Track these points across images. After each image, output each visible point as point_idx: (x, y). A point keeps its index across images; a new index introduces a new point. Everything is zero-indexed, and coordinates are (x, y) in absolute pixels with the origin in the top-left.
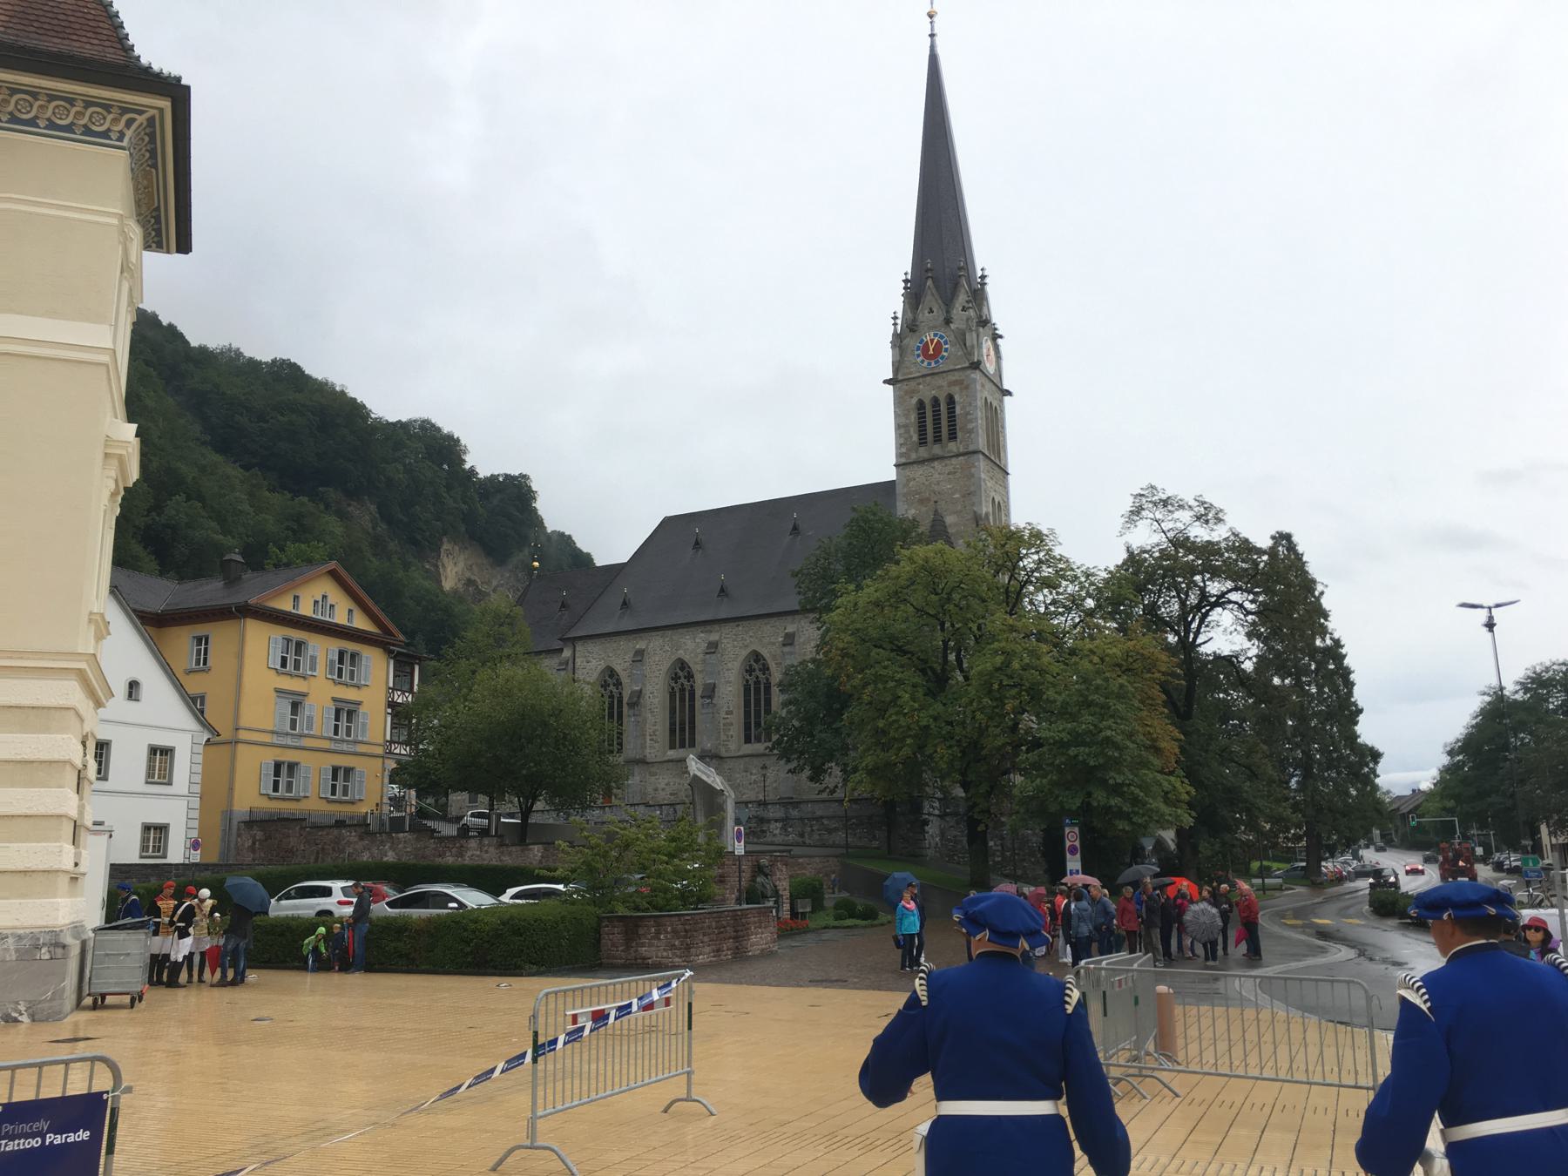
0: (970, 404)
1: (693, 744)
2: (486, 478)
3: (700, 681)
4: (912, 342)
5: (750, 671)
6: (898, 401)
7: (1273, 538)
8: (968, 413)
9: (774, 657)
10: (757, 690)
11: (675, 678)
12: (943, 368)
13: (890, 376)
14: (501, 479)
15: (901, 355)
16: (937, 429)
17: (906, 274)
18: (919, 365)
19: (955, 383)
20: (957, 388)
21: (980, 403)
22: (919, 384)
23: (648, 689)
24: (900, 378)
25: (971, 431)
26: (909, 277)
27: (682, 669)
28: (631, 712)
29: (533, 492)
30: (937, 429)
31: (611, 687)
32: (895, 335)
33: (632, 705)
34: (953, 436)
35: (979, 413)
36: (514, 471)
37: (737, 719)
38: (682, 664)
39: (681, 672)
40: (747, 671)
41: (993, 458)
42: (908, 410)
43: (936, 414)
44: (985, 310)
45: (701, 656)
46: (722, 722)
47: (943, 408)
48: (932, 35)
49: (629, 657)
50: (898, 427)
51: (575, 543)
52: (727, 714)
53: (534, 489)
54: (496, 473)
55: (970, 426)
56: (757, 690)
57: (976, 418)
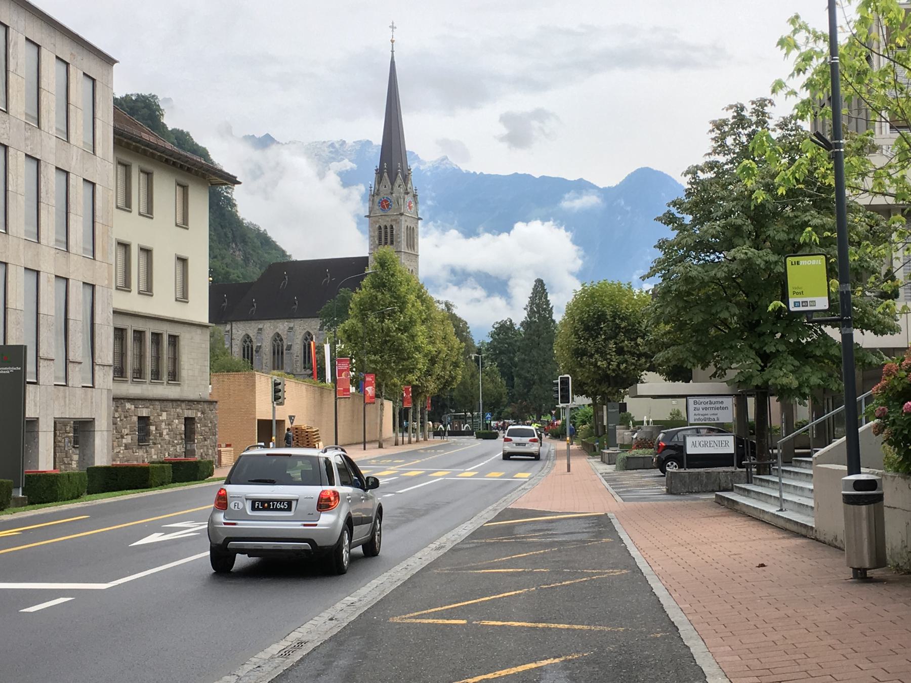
0: (399, 230)
1: (282, 369)
2: (122, 98)
3: (286, 343)
4: (377, 199)
6: (371, 225)
7: (536, 281)
8: (398, 234)
11: (275, 340)
13: (368, 214)
14: (134, 98)
16: (386, 239)
18: (379, 212)
19: (395, 220)
20: (394, 223)
21: (403, 229)
23: (263, 346)
24: (372, 215)
25: (399, 242)
26: (378, 167)
28: (257, 355)
29: (161, 110)
30: (386, 239)
31: (248, 343)
33: (257, 352)
34: (392, 243)
35: (403, 234)
36: (145, 92)
38: (278, 335)
39: (278, 338)
41: (410, 252)
43: (386, 233)
44: (409, 185)
45: (286, 332)
47: (389, 230)
48: (393, 51)
49: (256, 331)
50: (371, 236)
51: (192, 139)
52: (297, 356)
53: (162, 107)
54: (129, 93)
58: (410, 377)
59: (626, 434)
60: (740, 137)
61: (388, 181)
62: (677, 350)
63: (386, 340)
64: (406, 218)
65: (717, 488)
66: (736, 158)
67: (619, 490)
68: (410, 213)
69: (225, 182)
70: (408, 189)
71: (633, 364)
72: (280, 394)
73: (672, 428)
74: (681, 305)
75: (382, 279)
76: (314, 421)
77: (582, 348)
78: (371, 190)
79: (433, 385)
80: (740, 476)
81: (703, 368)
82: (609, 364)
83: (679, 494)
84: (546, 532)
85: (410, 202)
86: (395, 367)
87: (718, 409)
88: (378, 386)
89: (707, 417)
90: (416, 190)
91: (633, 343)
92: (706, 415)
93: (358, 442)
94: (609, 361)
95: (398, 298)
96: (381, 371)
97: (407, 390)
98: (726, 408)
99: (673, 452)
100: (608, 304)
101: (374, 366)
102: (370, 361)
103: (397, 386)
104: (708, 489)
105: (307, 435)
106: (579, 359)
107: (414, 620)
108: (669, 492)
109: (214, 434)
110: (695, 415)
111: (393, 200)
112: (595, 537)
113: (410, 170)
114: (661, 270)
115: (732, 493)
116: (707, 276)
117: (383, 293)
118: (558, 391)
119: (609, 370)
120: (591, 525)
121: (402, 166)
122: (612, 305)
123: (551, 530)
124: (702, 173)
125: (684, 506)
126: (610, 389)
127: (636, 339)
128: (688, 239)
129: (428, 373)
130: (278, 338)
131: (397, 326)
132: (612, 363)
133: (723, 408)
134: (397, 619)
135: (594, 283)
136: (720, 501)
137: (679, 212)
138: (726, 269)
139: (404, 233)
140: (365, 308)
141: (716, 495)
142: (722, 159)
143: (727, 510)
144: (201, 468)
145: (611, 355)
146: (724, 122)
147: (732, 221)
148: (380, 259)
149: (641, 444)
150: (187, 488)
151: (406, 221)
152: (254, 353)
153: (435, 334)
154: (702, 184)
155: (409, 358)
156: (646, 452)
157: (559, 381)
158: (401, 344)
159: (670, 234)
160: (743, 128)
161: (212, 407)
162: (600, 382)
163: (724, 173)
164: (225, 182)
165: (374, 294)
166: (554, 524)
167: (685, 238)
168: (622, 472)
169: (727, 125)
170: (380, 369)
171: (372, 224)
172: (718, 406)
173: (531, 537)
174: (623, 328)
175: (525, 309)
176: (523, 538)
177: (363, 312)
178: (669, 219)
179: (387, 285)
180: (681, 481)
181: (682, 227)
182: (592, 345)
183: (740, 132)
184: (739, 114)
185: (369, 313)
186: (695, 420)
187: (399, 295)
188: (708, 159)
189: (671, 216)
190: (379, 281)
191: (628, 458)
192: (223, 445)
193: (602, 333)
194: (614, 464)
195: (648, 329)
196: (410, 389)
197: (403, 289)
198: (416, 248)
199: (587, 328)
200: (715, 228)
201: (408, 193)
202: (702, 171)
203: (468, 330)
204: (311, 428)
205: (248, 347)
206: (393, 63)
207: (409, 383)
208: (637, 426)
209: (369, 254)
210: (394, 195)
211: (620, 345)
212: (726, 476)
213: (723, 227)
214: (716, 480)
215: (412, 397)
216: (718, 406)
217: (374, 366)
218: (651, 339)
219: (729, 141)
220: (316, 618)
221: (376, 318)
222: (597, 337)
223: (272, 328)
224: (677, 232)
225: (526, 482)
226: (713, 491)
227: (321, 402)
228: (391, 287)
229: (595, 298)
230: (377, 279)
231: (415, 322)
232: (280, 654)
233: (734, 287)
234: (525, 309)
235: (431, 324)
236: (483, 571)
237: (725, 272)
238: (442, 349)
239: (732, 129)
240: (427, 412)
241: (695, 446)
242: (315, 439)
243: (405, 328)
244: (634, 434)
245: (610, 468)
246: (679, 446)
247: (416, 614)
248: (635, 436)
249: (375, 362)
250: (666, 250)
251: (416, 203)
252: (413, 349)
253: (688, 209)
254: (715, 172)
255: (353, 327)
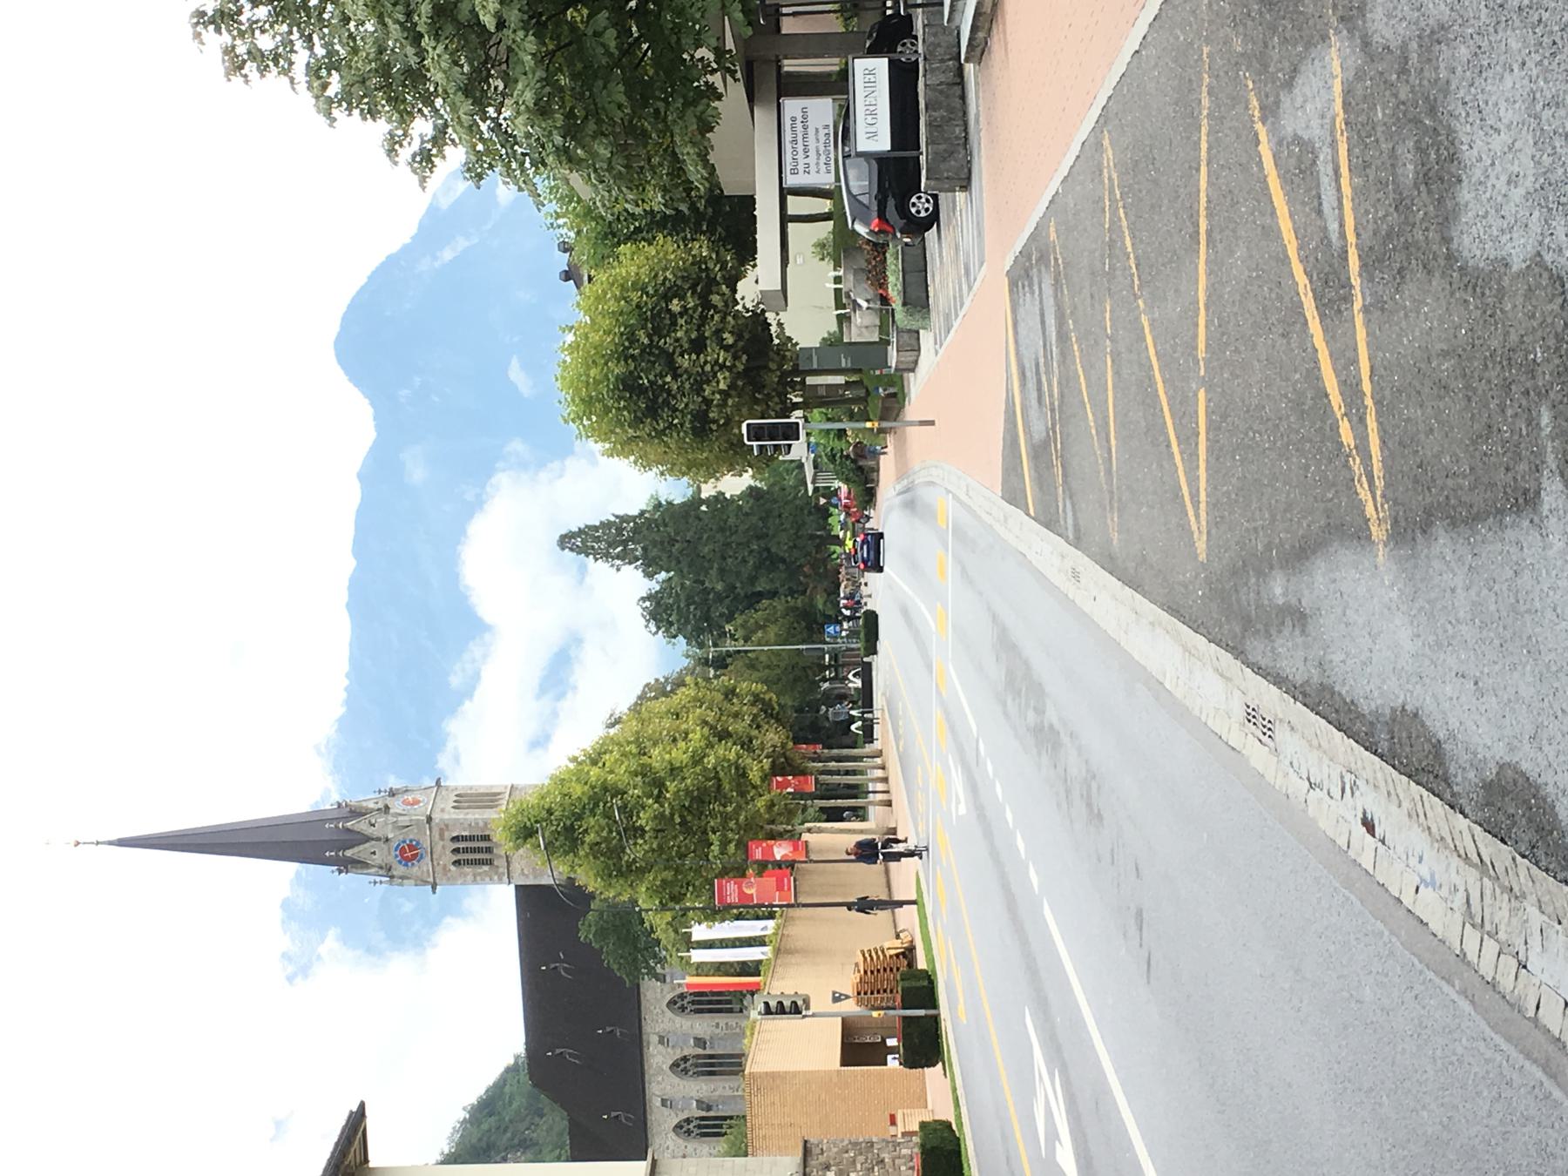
3: (690, 1050)
4: (399, 870)
5: (683, 1009)
6: (451, 880)
7: (563, 549)
8: (470, 825)
9: (673, 989)
10: (700, 1003)
11: (686, 1071)
12: (427, 844)
13: (430, 887)
15: (408, 878)
16: (479, 850)
17: (333, 872)
18: (426, 864)
20: (446, 834)
21: (460, 815)
22: (438, 864)
23: (694, 1094)
24: (431, 880)
27: (678, 1066)
28: (715, 1108)
30: (479, 850)
31: (691, 1126)
32: (391, 883)
34: (486, 838)
35: (469, 816)
37: (722, 1019)
38: (675, 1065)
39: (681, 1067)
40: (683, 1011)
42: (461, 873)
43: (466, 850)
44: (371, 805)
45: (669, 1050)
46: (725, 1031)
47: (461, 845)
48: (98, 843)
49: (666, 1111)
50: (474, 881)
55: (481, 824)
56: (700, 1003)
57: (475, 819)
58: (754, 775)
59: (859, 320)
60: (257, 22)
61: (361, 847)
62: (681, 135)
63: (679, 824)
64: (437, 810)
65: (958, 90)
66: (299, 28)
67: (965, 287)
68: (428, 803)
69: (360, 1133)
70: (376, 807)
71: (723, 320)
72: (787, 1003)
73: (844, 208)
74: (591, 126)
75: (559, 833)
76: (843, 964)
77: (691, 422)
78: (381, 882)
79: (770, 735)
80: (932, 43)
81: (719, 97)
82: (722, 367)
83: (969, 162)
84: (1042, 369)
85: (406, 803)
86: (734, 805)
87: (805, 128)
88: (773, 836)
89: (822, 149)
90: (380, 792)
91: (681, 321)
92: (818, 151)
93: (885, 884)
94: (717, 368)
95: (595, 800)
96: (742, 832)
97: (780, 785)
98: (804, 112)
99: (891, 203)
100: (603, 369)
101: (732, 848)
102: (722, 854)
103: (772, 801)
104: (958, 106)
105: (872, 972)
106: (714, 427)
107: (1203, 506)
108: (966, 185)
109: (872, 1144)
110: (818, 172)
111: (401, 838)
112: (1047, 266)
113: (339, 805)
114: (523, 171)
115: (963, 27)
116: (534, 74)
117: (586, 831)
118: (775, 446)
119: (734, 366)
120: (1027, 289)
121: (331, 820)
122: (606, 364)
123: (1037, 365)
124: (330, 87)
125: (988, 123)
126: (773, 366)
127: (673, 316)
128: (461, 113)
129: (747, 744)
130: (681, 1067)
131: (651, 801)
132: (721, 361)
133: (805, 118)
134: (1201, 545)
135: (563, 400)
136: (979, 50)
137: (410, 144)
138: (521, 34)
139: (468, 813)
140: (615, 865)
141: (967, 60)
142: (301, 58)
143: (994, 25)
144: (935, 1143)
145: (706, 362)
146: (229, 51)
147: (425, 23)
148: (517, 839)
149: (878, 279)
150: (973, 1162)
151: (443, 810)
152: (712, 1114)
153: (669, 732)
154: (352, 86)
155: (717, 777)
156: (893, 267)
157: (755, 444)
158: (688, 792)
159: (455, 156)
160: (239, 12)
161: (816, 1151)
162: (759, 387)
163: (331, 53)
164: (360, 1133)
165: (586, 847)
166: (1027, 366)
167: (459, 118)
168: (933, 314)
169: (233, 47)
170: (738, 833)
171: (449, 879)
172: (799, 126)
173: (1051, 396)
174: (652, 341)
175: (618, 570)
176: (1053, 410)
177: (624, 869)
178: (425, 159)
179: (568, 823)
180: (944, 159)
181: (439, 138)
182: (685, 400)
183: (248, 20)
184: (212, 22)
185: (626, 858)
186: (828, 172)
187: (590, 798)
188: (302, 87)
189: (418, 159)
190: (562, 838)
191: (904, 304)
192: (892, 1130)
193: (660, 382)
194: (918, 332)
195: (650, 290)
196: (779, 779)
197: (578, 790)
198: (494, 791)
199: (652, 412)
200: (439, 56)
201: (387, 808)
202: (325, 86)
203: (662, 680)
204: (857, 965)
205: (699, 1127)
206: (123, 843)
207: (765, 778)
208: (844, 300)
209: (509, 883)
210: (390, 836)
211: (686, 346)
212: (933, 70)
213: (438, 41)
214: (941, 92)
215: (794, 775)
216: (799, 126)
217: (732, 848)
218: (663, 197)
219: (265, 42)
220: (1203, 719)
221: (635, 844)
222: (669, 391)
223: (660, 1079)
224: (448, 150)
225: (955, 497)
226: (961, 65)
227: (799, 918)
228: (574, 814)
229: (591, 397)
230: (557, 844)
231: (643, 765)
232: (1265, 739)
233: (557, 25)
234: (618, 570)
235: (649, 740)
236: (1113, 442)
237: (526, 36)
238: (699, 718)
239: (242, 34)
240: (826, 751)
241: (875, 134)
242: (878, 957)
243: (656, 785)
244: (860, 306)
245: (926, 339)
246: (879, 191)
247: (1191, 513)
248: (864, 305)
249: (724, 844)
250: (486, 166)
251: (407, 791)
252: (698, 769)
253: (402, 116)
254: (329, 74)
255: (656, 891)
